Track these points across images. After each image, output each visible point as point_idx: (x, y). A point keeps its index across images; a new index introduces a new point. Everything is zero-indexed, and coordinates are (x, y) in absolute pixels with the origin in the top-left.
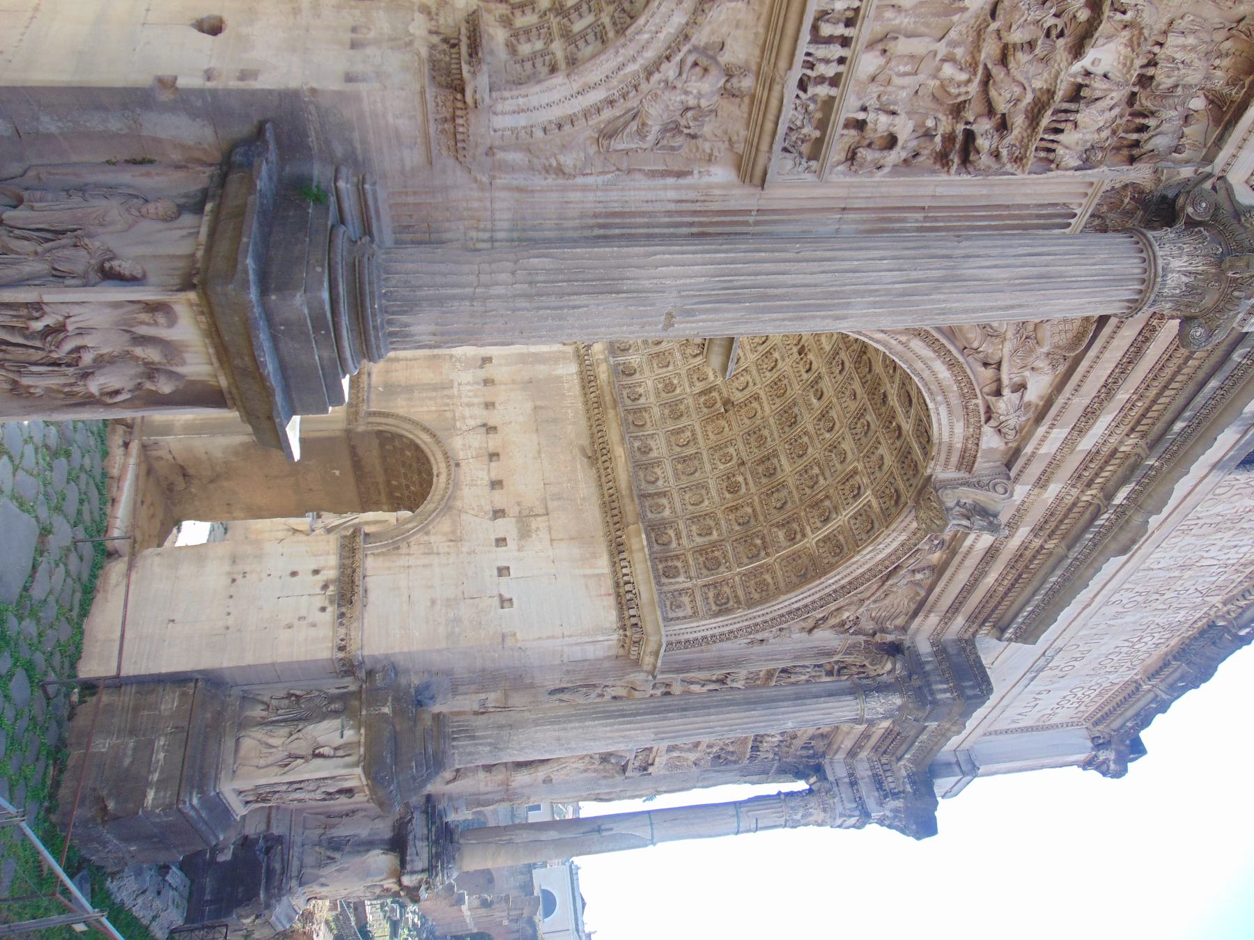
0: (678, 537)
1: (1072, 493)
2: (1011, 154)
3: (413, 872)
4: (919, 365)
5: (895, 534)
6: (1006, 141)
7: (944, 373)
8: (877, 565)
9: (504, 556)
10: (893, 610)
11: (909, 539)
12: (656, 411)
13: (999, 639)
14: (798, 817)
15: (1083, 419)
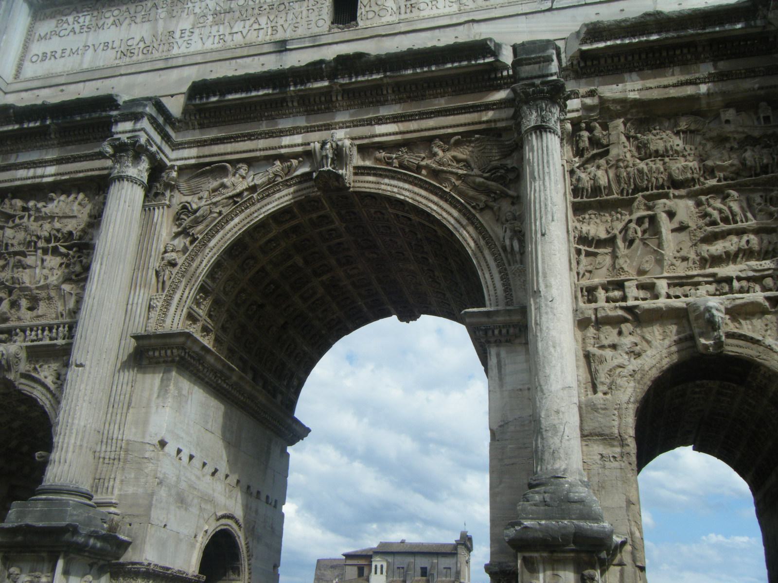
4: (229, 235)
5: (383, 187)
7: (237, 220)
8: (415, 185)
10: (489, 147)
13: (497, 60)
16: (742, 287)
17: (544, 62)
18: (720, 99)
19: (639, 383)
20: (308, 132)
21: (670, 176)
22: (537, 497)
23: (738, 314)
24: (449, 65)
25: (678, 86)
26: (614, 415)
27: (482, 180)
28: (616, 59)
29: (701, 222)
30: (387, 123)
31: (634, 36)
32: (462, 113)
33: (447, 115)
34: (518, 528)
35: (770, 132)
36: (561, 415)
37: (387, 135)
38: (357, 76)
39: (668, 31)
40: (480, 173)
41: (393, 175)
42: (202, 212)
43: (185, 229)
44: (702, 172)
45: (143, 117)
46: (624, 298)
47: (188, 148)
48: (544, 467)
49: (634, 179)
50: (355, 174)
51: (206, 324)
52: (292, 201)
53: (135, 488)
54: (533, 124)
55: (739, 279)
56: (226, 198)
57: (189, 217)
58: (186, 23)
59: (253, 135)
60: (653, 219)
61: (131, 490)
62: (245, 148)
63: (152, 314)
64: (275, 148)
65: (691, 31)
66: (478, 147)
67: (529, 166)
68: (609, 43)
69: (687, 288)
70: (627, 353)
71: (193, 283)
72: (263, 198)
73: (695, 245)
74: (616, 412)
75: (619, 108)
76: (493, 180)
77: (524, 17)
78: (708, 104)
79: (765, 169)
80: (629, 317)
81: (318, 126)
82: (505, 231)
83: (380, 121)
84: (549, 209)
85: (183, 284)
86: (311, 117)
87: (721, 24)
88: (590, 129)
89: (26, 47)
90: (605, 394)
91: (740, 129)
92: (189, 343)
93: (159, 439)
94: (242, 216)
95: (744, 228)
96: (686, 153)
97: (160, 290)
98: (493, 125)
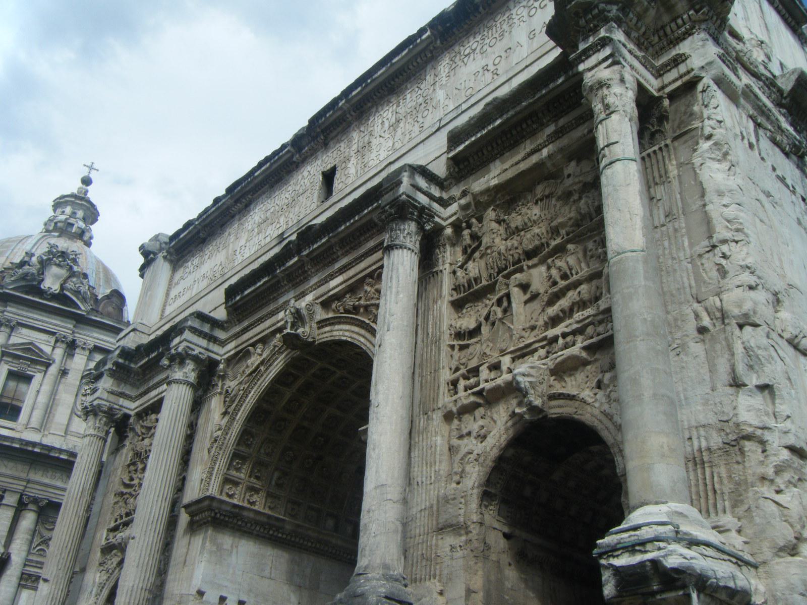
5: (335, 333)
7: (252, 393)
16: (567, 343)
18: (560, 156)
19: (482, 466)
23: (564, 373)
24: (366, 211)
25: (526, 158)
26: (461, 503)
30: (337, 277)
31: (483, 128)
36: (371, 514)
38: (313, 245)
44: (550, 235)
50: (319, 328)
51: (251, 484)
58: (242, 242)
59: (263, 318)
68: (467, 143)
70: (475, 438)
72: (267, 369)
74: (463, 500)
75: (486, 198)
77: (422, 144)
78: (554, 165)
84: (386, 321)
88: (469, 226)
89: (167, 295)
90: (458, 483)
91: (577, 180)
92: (215, 504)
93: (196, 589)
95: (578, 280)
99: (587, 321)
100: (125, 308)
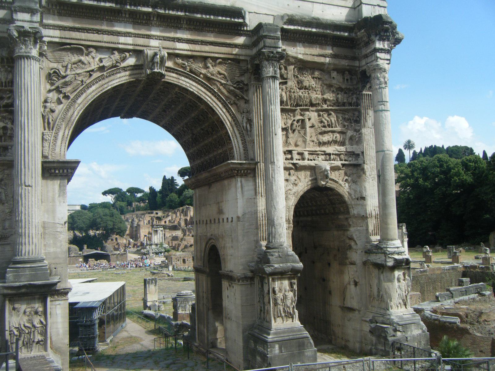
0: (221, 153)
1: (155, 22)
2: (8, 94)
3: (386, 261)
4: (90, 97)
5: (181, 82)
6: (4, 96)
7: (94, 88)
8: (199, 84)
9: (225, 220)
10: (234, 68)
11: (183, 76)
12: (202, 160)
13: (245, 22)
14: (378, 82)
15: (114, 34)
17: (276, 39)
18: (332, 66)
20: (136, 37)
21: (311, 100)
22: (277, 254)
27: (233, 88)
28: (295, 35)
29: (320, 125)
30: (183, 43)
31: (306, 27)
32: (223, 46)
33: (215, 46)
34: (273, 268)
35: (348, 87)
37: (183, 50)
39: (319, 28)
40: (232, 84)
41: (187, 76)
42: (70, 79)
43: (58, 87)
45: (37, 12)
46: (292, 159)
47: (52, 29)
48: (276, 241)
49: (297, 100)
52: (128, 80)
53: (55, 249)
54: (271, 75)
55: (333, 154)
56: (85, 72)
57: (59, 80)
60: (303, 121)
61: (52, 250)
62: (94, 39)
63: (46, 144)
64: (115, 43)
65: (328, 31)
66: (229, 67)
67: (268, 96)
69: (315, 156)
71: (70, 126)
72: (110, 76)
73: (317, 135)
75: (293, 61)
76: (237, 89)
78: (328, 68)
79: (344, 104)
80: (294, 167)
81: (142, 35)
82: (243, 118)
83: (180, 40)
85: (63, 126)
86: (136, 26)
87: (340, 31)
94: (97, 86)
96: (316, 90)
97: (47, 128)
98: (238, 57)
99: (342, 153)
100: (396, 178)
